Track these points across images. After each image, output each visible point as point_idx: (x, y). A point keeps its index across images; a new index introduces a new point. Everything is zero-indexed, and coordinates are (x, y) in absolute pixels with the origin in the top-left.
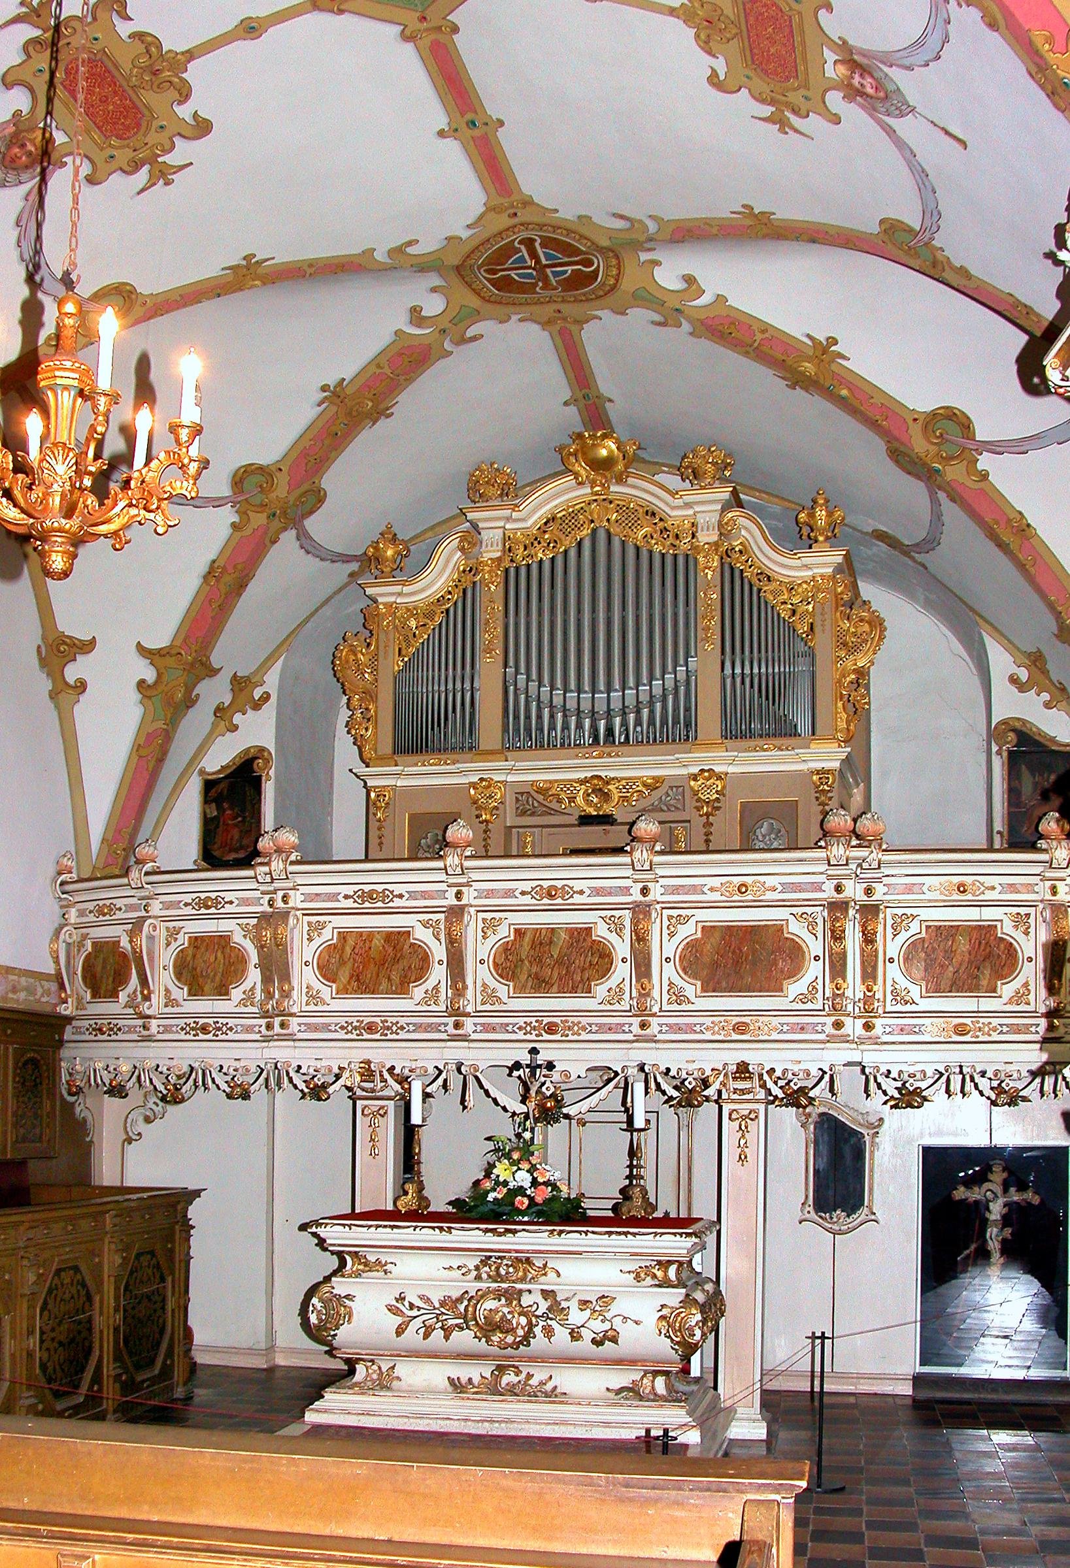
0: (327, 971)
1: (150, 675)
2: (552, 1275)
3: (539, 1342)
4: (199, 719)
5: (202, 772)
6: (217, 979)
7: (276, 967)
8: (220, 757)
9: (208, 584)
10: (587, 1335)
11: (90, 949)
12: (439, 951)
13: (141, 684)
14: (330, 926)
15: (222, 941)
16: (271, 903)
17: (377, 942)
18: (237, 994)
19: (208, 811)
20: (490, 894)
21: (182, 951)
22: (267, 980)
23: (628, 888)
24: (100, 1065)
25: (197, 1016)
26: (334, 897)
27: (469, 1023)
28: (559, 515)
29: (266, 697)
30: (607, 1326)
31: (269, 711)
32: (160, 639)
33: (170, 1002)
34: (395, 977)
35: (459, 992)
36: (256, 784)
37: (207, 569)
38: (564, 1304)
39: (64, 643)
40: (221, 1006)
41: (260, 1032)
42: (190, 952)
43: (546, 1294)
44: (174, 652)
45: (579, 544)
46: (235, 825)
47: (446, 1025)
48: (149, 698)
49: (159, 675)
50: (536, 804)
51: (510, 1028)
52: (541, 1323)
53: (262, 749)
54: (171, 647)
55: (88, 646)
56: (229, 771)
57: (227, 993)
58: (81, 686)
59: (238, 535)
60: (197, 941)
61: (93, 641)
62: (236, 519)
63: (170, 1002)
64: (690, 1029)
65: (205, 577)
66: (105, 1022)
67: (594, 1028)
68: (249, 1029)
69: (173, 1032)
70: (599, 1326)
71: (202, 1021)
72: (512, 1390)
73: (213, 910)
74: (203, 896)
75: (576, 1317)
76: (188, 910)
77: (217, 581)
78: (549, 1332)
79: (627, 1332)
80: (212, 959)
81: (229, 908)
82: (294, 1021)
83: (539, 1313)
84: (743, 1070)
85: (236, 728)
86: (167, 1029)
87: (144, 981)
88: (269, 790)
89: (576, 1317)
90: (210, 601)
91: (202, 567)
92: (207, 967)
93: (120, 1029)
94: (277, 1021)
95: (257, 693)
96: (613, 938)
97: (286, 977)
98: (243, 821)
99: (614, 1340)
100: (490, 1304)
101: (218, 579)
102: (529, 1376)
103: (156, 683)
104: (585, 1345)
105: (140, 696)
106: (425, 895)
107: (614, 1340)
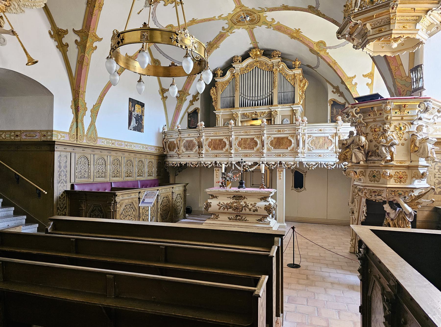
0: (209, 146)
3: (244, 211)
7: (200, 146)
12: (227, 143)
15: (192, 141)
16: (200, 135)
17: (217, 141)
18: (194, 150)
20: (236, 133)
22: (199, 148)
24: (171, 163)
25: (187, 154)
26: (210, 133)
31: (199, 100)
34: (220, 147)
36: (197, 114)
40: (191, 152)
43: (245, 202)
58: (167, 97)
60: (187, 141)
64: (271, 156)
70: (254, 208)
72: (239, 220)
75: (250, 207)
78: (245, 210)
82: (203, 155)
84: (281, 163)
87: (178, 148)
89: (250, 207)
92: (189, 146)
94: (201, 155)
96: (257, 140)
97: (202, 147)
99: (257, 211)
102: (242, 217)
104: (252, 212)
106: (226, 133)
107: (257, 211)
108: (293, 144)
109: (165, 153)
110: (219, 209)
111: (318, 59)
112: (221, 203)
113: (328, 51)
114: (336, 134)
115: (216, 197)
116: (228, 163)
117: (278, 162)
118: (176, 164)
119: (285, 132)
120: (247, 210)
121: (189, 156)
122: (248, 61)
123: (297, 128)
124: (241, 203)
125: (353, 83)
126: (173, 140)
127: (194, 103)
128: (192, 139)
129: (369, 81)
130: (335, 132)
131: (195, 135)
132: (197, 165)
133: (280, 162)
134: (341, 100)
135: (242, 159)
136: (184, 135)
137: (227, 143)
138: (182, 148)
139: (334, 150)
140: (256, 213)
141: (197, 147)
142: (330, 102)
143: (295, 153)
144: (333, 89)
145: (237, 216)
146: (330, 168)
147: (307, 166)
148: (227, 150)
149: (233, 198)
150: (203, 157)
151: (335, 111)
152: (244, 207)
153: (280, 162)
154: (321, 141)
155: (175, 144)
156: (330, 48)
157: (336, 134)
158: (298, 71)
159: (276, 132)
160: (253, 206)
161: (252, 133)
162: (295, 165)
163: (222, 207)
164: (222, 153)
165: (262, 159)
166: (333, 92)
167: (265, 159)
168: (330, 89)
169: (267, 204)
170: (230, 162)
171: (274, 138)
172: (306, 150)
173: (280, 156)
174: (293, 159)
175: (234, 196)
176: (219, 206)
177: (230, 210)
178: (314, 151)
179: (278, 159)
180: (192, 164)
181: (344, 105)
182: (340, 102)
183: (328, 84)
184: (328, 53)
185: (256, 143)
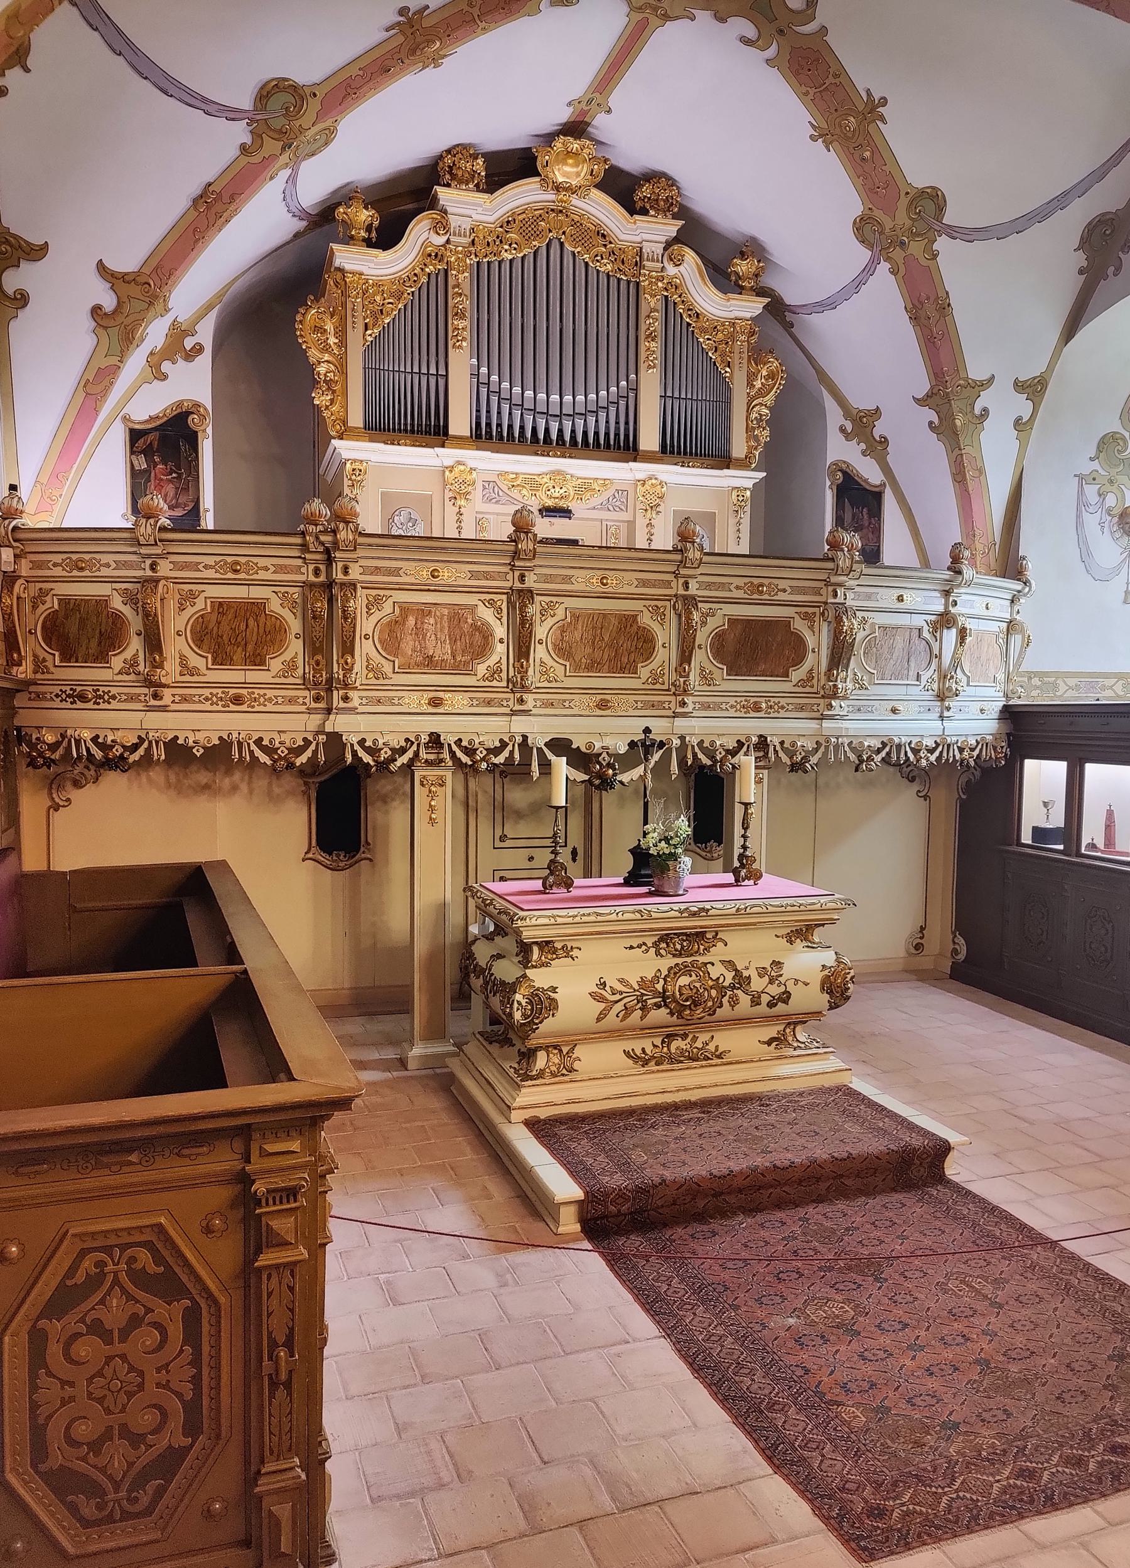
1: (108, 302)
2: (720, 945)
4: (136, 362)
5: (126, 419)
6: (250, 648)
7: (329, 636)
8: (151, 404)
9: (196, 209)
10: (765, 999)
11: (56, 606)
13: (96, 311)
14: (390, 602)
15: (257, 608)
16: (317, 572)
18: (276, 665)
19: (136, 463)
20: (548, 579)
21: (202, 616)
22: (316, 647)
23: (669, 582)
27: (529, 698)
28: (521, 217)
29: (198, 349)
30: (782, 989)
32: (127, 262)
33: (186, 668)
35: (523, 672)
36: (193, 440)
37: (199, 192)
38: (745, 973)
39: (7, 242)
40: (255, 676)
41: (304, 704)
42: (214, 617)
44: (140, 280)
45: (535, 253)
46: (170, 481)
47: (508, 700)
48: (105, 328)
49: (120, 304)
50: (501, 493)
51: (567, 704)
52: (729, 993)
53: (197, 405)
54: (139, 273)
55: (37, 252)
56: (158, 423)
57: (262, 663)
59: (244, 160)
60: (221, 607)
61: (44, 249)
62: (247, 139)
63: (186, 668)
64: (718, 707)
65: (195, 201)
66: (90, 688)
67: (640, 705)
68: (291, 701)
69: (194, 702)
70: (775, 990)
71: (232, 691)
73: (242, 576)
74: (229, 559)
75: (757, 984)
76: (211, 574)
77: (208, 208)
79: (796, 992)
80: (243, 626)
81: (262, 575)
83: (726, 984)
84: (762, 744)
85: (164, 377)
86: (185, 699)
88: (206, 448)
90: (195, 230)
91: (194, 188)
92: (236, 635)
93: (114, 697)
95: (189, 343)
96: (655, 627)
97: (348, 648)
98: (179, 477)
100: (684, 980)
101: (209, 206)
102: (695, 1039)
103: (115, 311)
104: (763, 1008)
105: (94, 324)
106: (487, 576)
107: (786, 1002)
108: (810, 655)
109: (24, 671)
110: (598, 1020)
111: (869, 270)
112: (612, 982)
113: (942, 244)
114: (945, 620)
115: (567, 952)
116: (504, 745)
117: (755, 739)
118: (135, 747)
119: (782, 596)
120: (744, 999)
121: (237, 700)
122: (523, 195)
123: (834, 579)
124: (715, 971)
125: (977, 411)
126: (103, 590)
127: (166, 366)
128: (257, 593)
129: (1024, 408)
130: (941, 608)
131: (279, 569)
132: (300, 751)
133: (763, 739)
134: (870, 472)
135: (647, 731)
136: (195, 567)
137: (500, 631)
138: (177, 647)
139: (935, 686)
140: (781, 1008)
141: (295, 648)
142: (832, 474)
143: (823, 696)
144: (843, 421)
145: (671, 1037)
146: (924, 763)
147: (853, 757)
148: (494, 673)
149: (656, 945)
150: (353, 710)
151: (848, 517)
152: (732, 987)
153: (763, 739)
154: (900, 642)
155: (117, 618)
156: (953, 232)
157: (945, 620)
158: (749, 307)
159: (740, 594)
160: (771, 982)
161: (627, 589)
162: (819, 754)
163: (619, 1007)
164: (465, 689)
165: (679, 722)
166: (842, 430)
167: (693, 722)
168: (834, 417)
169: (828, 958)
170: (519, 739)
171: (733, 622)
172: (850, 685)
173: (757, 709)
174: (814, 724)
175: (662, 939)
176: (599, 998)
177: (660, 1015)
178: (873, 690)
179: (753, 727)
180: (266, 750)
181: (878, 496)
182: (866, 481)
183: (825, 393)
184: (935, 256)
185: (645, 644)
